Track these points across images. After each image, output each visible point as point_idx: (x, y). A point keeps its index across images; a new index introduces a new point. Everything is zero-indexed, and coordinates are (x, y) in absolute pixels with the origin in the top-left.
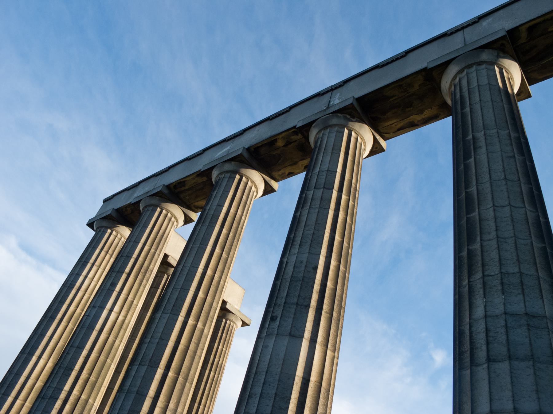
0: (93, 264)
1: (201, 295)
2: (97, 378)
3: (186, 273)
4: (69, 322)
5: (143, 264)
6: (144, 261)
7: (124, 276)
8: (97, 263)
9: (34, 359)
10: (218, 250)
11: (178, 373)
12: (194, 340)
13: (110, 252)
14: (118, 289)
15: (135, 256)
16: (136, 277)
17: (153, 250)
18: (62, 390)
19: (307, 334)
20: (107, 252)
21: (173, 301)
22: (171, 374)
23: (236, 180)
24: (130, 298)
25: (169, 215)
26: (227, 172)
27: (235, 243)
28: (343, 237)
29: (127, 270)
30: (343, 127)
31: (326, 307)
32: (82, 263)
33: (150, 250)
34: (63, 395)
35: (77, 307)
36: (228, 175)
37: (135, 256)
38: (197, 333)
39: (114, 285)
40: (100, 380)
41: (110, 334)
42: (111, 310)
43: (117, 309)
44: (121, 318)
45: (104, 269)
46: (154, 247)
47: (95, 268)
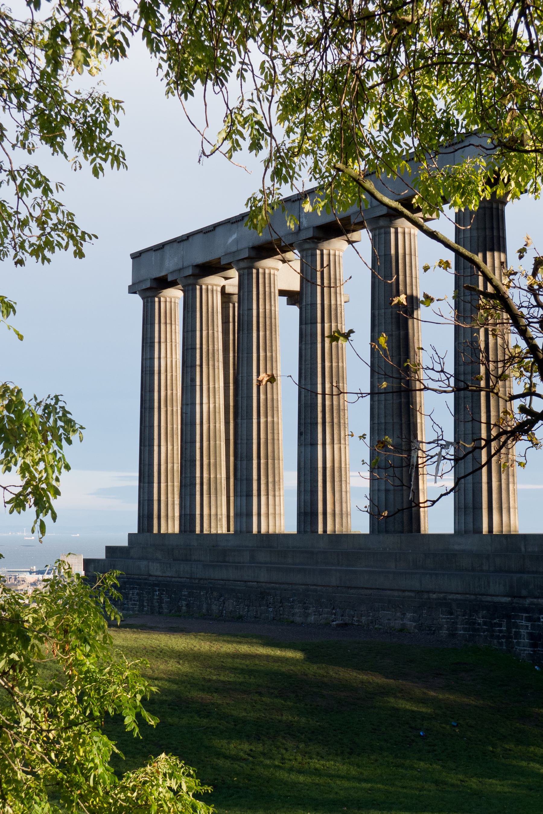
0: (160, 342)
1: (262, 397)
2: (216, 459)
3: (245, 382)
4: (167, 407)
5: (208, 350)
6: (208, 346)
7: (198, 369)
8: (163, 340)
9: (156, 448)
10: (262, 354)
11: (267, 458)
12: (269, 431)
13: (168, 321)
14: (198, 383)
15: (198, 346)
16: (208, 365)
17: (210, 332)
18: (195, 477)
19: (320, 441)
20: (166, 323)
21: (245, 408)
22: (262, 461)
23: (254, 276)
24: (211, 386)
25: (210, 287)
26: (244, 268)
27: (274, 336)
28: (331, 362)
29: (198, 362)
30: (315, 249)
31: (328, 419)
32: (149, 344)
33: (208, 333)
34: (198, 481)
35: (166, 390)
36: (246, 271)
37: (198, 346)
38: (269, 425)
39: (193, 380)
40: (218, 459)
41: (209, 423)
42: (201, 404)
43: (205, 400)
44: (212, 406)
45: (172, 342)
46: (210, 328)
47: (163, 345)
